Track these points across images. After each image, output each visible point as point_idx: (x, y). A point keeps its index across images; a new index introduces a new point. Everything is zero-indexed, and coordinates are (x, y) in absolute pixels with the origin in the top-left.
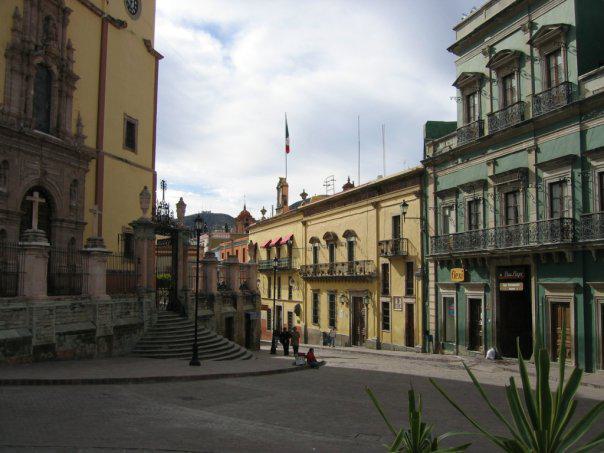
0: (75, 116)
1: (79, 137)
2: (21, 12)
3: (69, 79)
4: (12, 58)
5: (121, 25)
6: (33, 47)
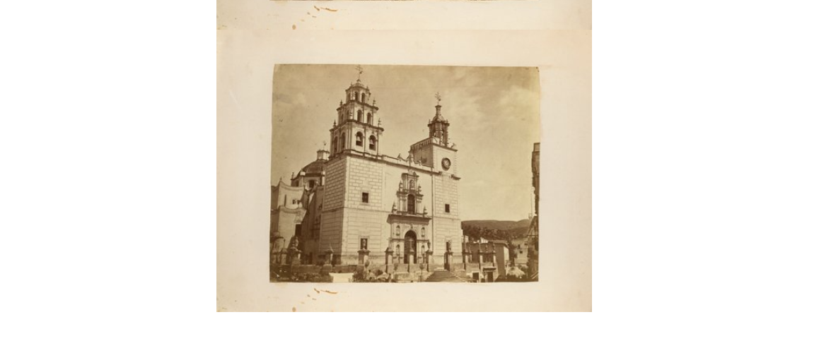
1: (425, 213)
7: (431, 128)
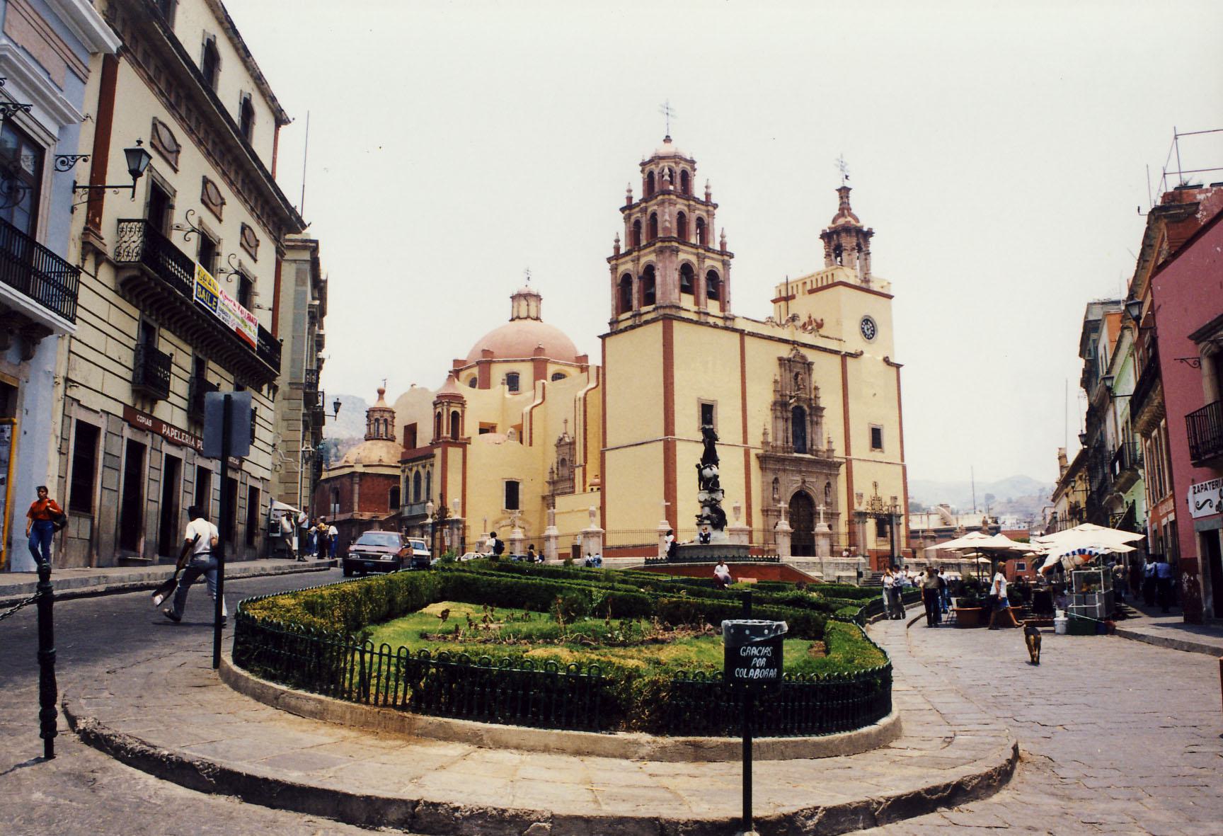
0: (825, 436)
1: (831, 451)
2: (778, 378)
3: (818, 411)
4: (775, 410)
5: (856, 356)
6: (788, 398)
7: (828, 244)
